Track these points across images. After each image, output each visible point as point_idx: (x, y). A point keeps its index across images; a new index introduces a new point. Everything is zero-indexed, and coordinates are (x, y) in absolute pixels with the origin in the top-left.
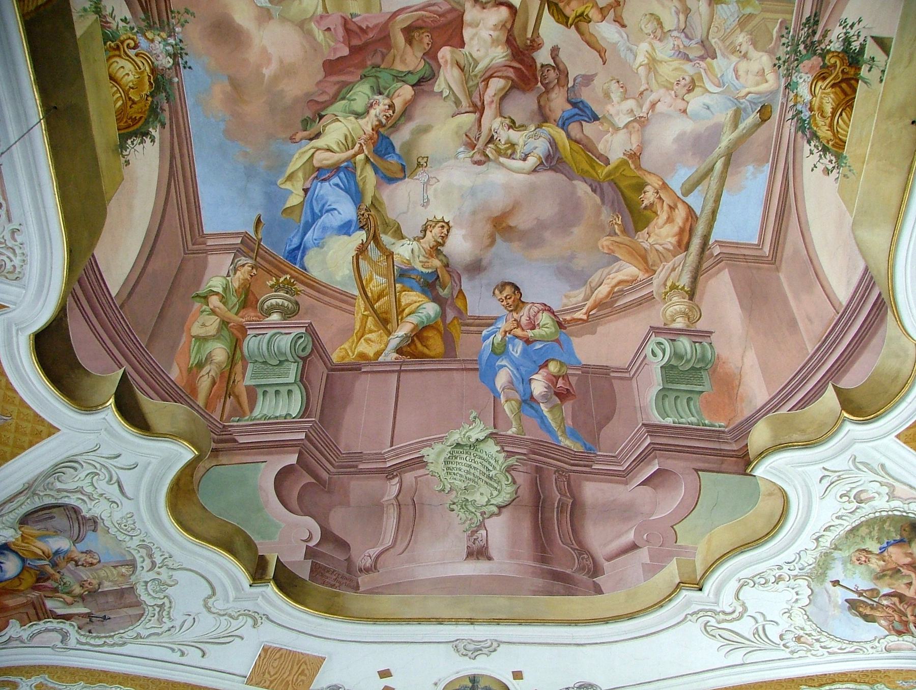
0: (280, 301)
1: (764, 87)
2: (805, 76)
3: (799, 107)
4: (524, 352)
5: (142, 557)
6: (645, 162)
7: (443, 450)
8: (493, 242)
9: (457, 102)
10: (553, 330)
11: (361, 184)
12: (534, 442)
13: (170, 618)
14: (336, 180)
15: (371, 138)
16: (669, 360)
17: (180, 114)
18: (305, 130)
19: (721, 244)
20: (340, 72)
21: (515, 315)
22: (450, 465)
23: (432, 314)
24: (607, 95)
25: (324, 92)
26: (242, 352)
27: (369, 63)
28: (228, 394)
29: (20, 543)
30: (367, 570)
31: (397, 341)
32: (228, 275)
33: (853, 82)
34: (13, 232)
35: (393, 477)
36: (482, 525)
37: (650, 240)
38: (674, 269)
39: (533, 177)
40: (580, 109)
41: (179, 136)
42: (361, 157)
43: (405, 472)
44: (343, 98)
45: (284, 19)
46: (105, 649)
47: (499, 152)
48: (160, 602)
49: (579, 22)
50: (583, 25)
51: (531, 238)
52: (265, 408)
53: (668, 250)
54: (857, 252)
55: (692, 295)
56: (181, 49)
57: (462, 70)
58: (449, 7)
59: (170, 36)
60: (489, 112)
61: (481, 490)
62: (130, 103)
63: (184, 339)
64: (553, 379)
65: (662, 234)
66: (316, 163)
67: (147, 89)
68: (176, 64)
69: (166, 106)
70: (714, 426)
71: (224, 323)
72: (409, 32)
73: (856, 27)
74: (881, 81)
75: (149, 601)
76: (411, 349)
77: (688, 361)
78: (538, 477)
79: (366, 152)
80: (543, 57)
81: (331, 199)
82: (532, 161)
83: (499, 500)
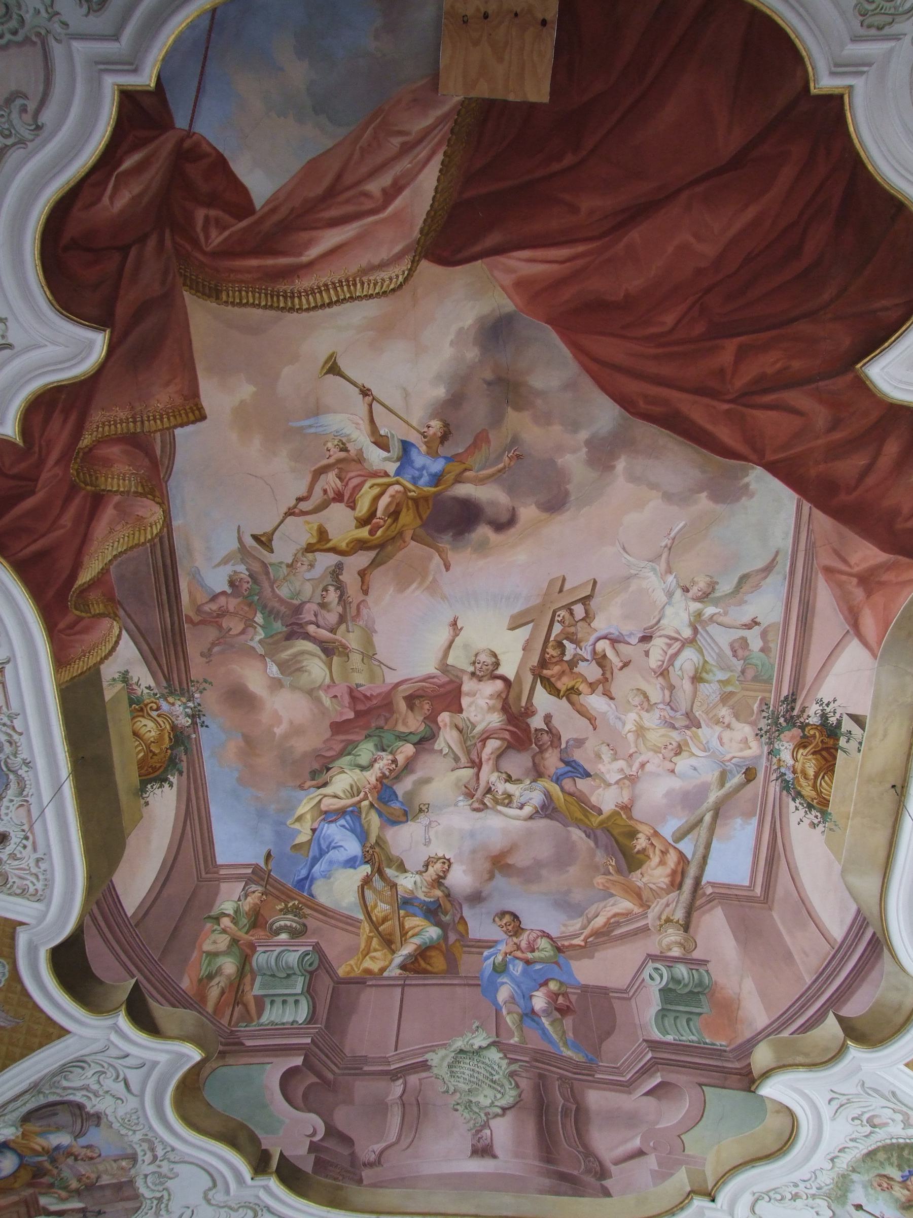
0: (288, 923)
1: (747, 753)
2: (786, 745)
3: (783, 770)
4: (525, 972)
5: (143, 1150)
6: (637, 813)
7: (447, 1056)
8: (492, 877)
9: (457, 759)
10: (552, 953)
11: (366, 826)
12: (536, 1051)
13: (167, 1211)
14: (342, 822)
15: (375, 788)
16: (667, 983)
17: (197, 765)
18: (313, 779)
19: (713, 885)
20: (346, 732)
21: (515, 940)
22: (454, 1069)
23: (435, 937)
24: (598, 756)
25: (331, 749)
26: (250, 963)
27: (373, 725)
28: (237, 1002)
30: (370, 1165)
31: (401, 959)
32: (239, 900)
33: (832, 750)
34: (38, 861)
35: (398, 1079)
36: (486, 1125)
37: (644, 880)
38: (668, 905)
39: (530, 823)
40: (573, 767)
41: (195, 781)
42: (365, 803)
43: (410, 1074)
44: (349, 754)
45: (294, 688)
47: (496, 802)
48: (158, 1195)
49: (571, 694)
50: (574, 697)
51: (529, 875)
52: (272, 1015)
53: (662, 889)
54: (848, 895)
55: (686, 927)
56: (199, 711)
57: (461, 731)
58: (448, 679)
59: (189, 701)
60: (486, 768)
61: (485, 1093)
62: (151, 755)
63: (195, 954)
64: (553, 997)
65: (655, 874)
66: (323, 807)
67: (167, 743)
68: (194, 723)
69: (184, 758)
70: (715, 1045)
71: (235, 941)
72: (411, 700)
73: (832, 705)
74: (859, 751)
76: (416, 965)
77: (686, 985)
78: (541, 1086)
79: (370, 798)
80: (537, 722)
81: (337, 838)
82: (528, 810)
83: (503, 1102)
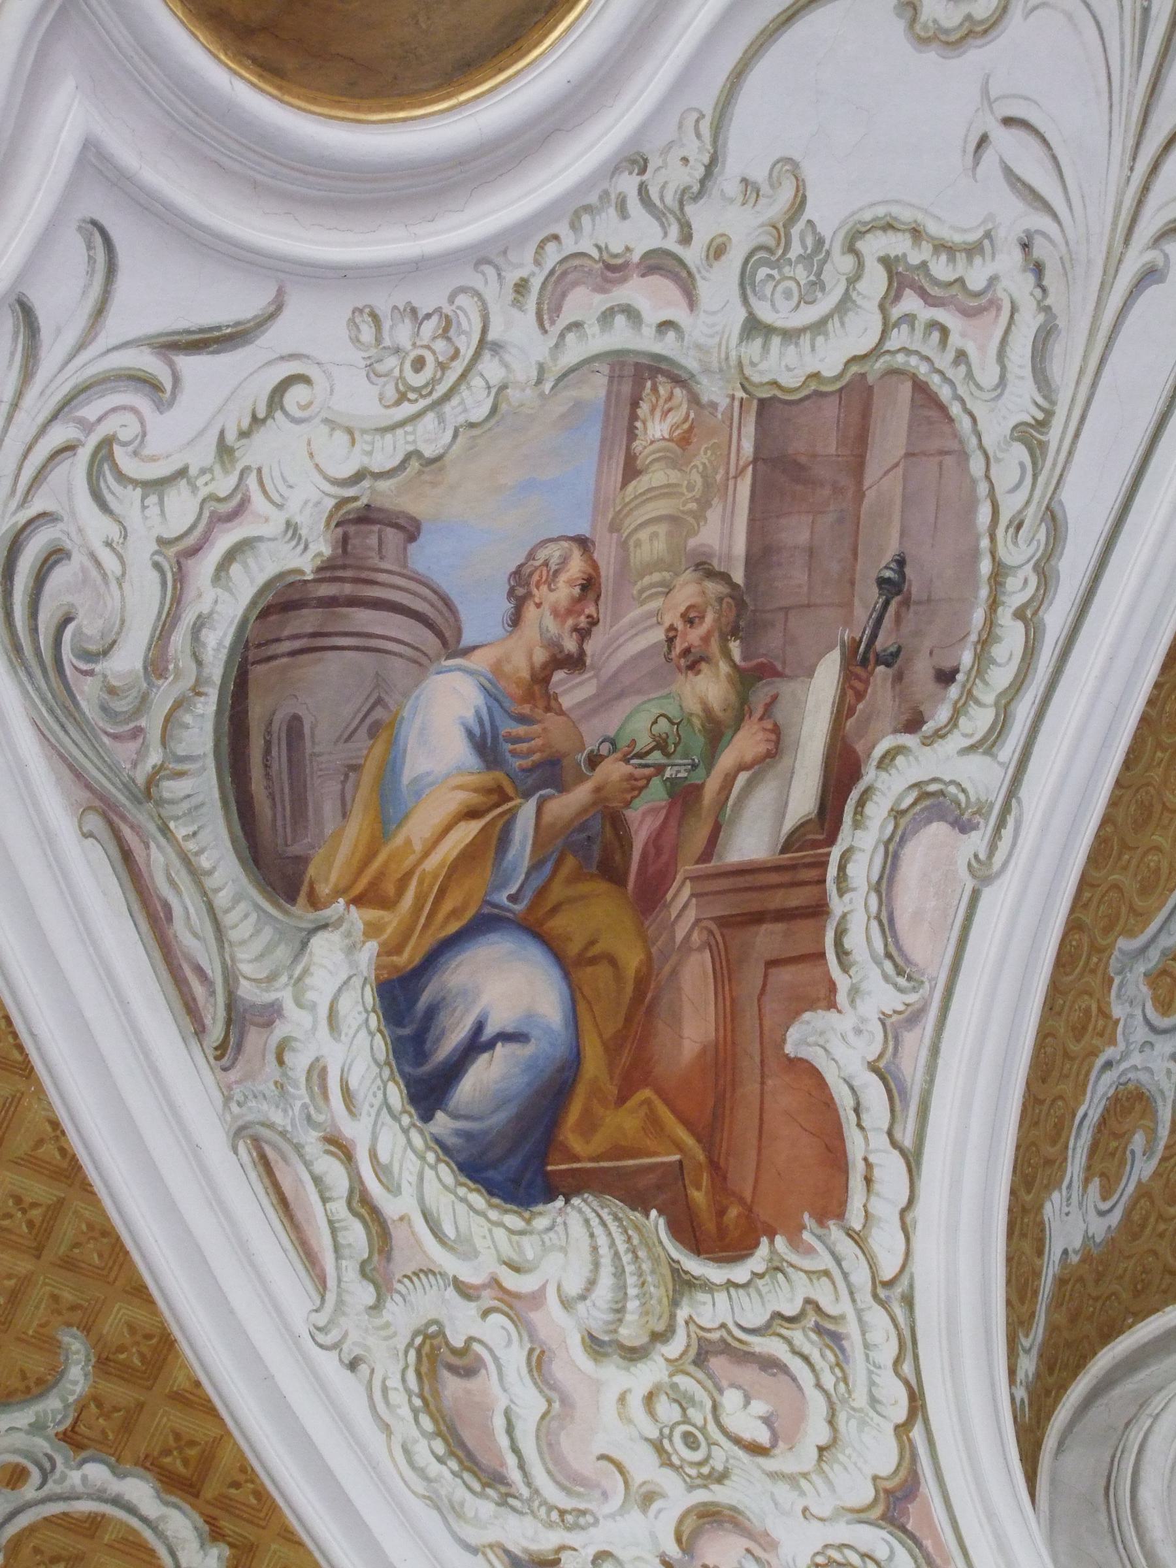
5: (607, 317)
13: (973, 250)
29: (392, 920)
46: (1055, 619)
48: (875, 282)
75: (858, 334)
